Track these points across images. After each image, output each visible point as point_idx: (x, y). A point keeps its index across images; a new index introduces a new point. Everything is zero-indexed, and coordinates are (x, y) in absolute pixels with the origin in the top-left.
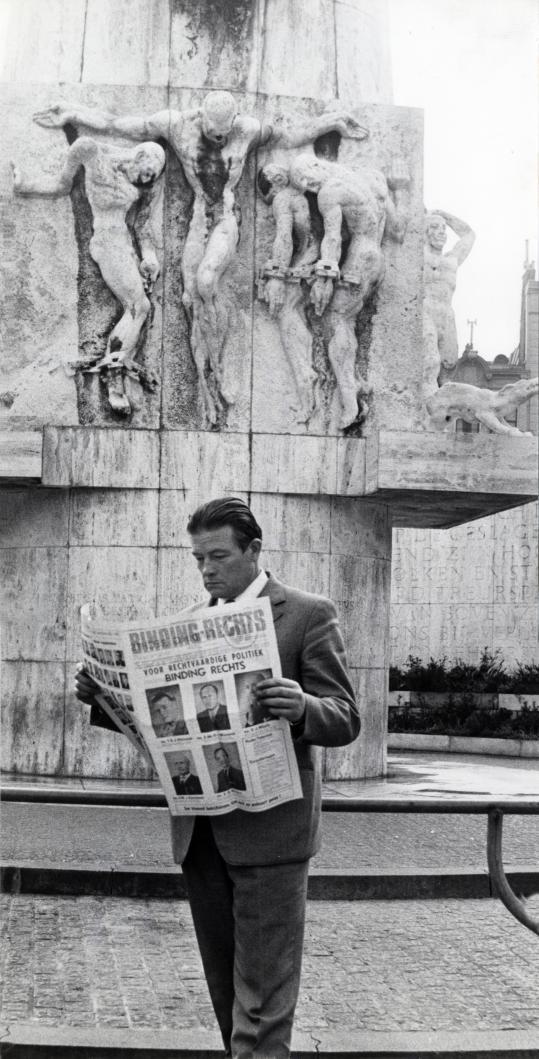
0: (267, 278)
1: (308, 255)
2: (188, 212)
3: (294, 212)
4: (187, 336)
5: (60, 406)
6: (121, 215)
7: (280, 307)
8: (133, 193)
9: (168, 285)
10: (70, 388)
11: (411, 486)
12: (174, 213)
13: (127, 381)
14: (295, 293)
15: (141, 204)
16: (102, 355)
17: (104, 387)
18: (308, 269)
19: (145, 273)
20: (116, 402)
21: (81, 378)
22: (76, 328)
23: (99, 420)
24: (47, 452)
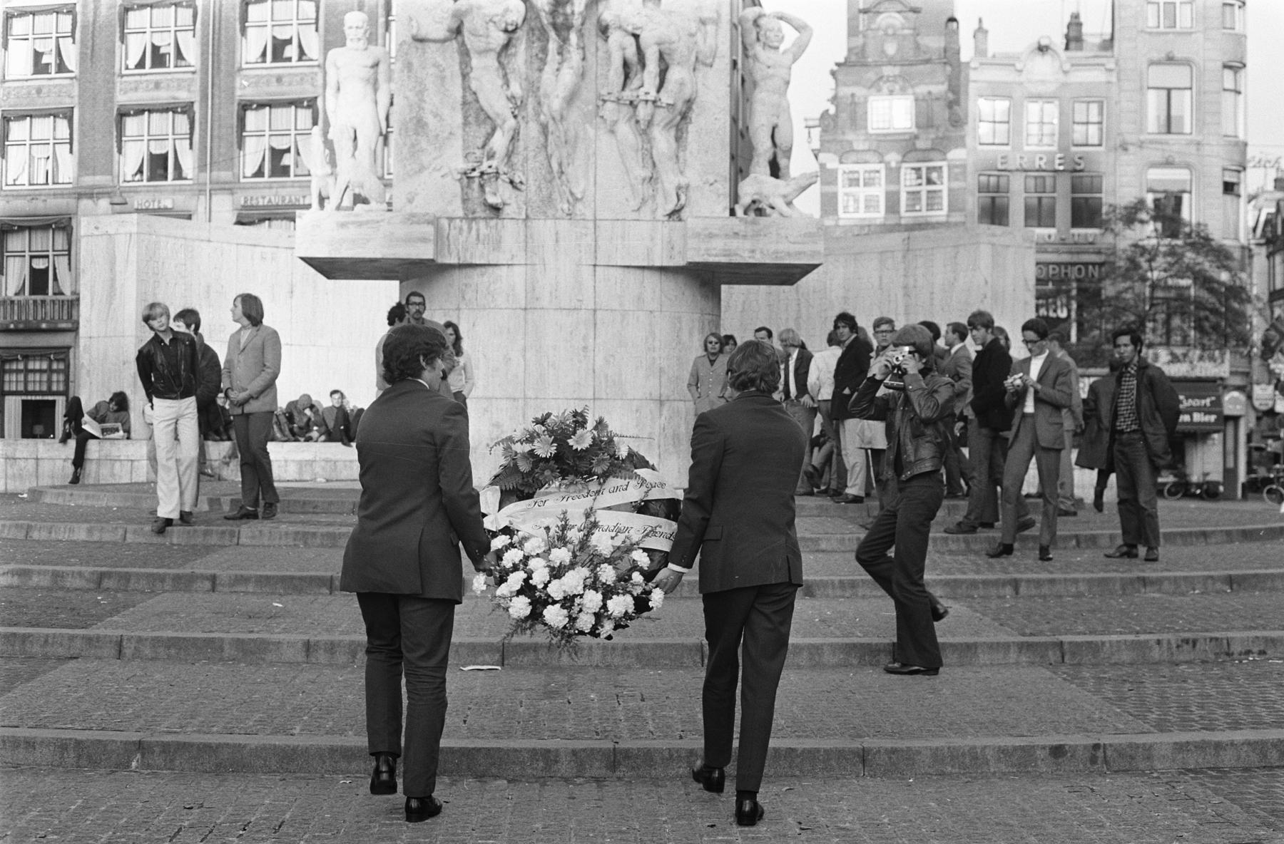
0: (604, 101)
1: (635, 83)
2: (544, 50)
3: (624, 49)
4: (546, 147)
5: (450, 203)
6: (493, 56)
7: (615, 122)
8: (501, 38)
9: (530, 107)
10: (457, 188)
11: (711, 260)
12: (535, 51)
13: (500, 181)
14: (626, 110)
15: (506, 46)
16: (481, 162)
17: (482, 186)
18: (635, 94)
19: (511, 98)
20: (492, 200)
21: (465, 180)
22: (460, 142)
23: (480, 212)
24: (440, 239)
